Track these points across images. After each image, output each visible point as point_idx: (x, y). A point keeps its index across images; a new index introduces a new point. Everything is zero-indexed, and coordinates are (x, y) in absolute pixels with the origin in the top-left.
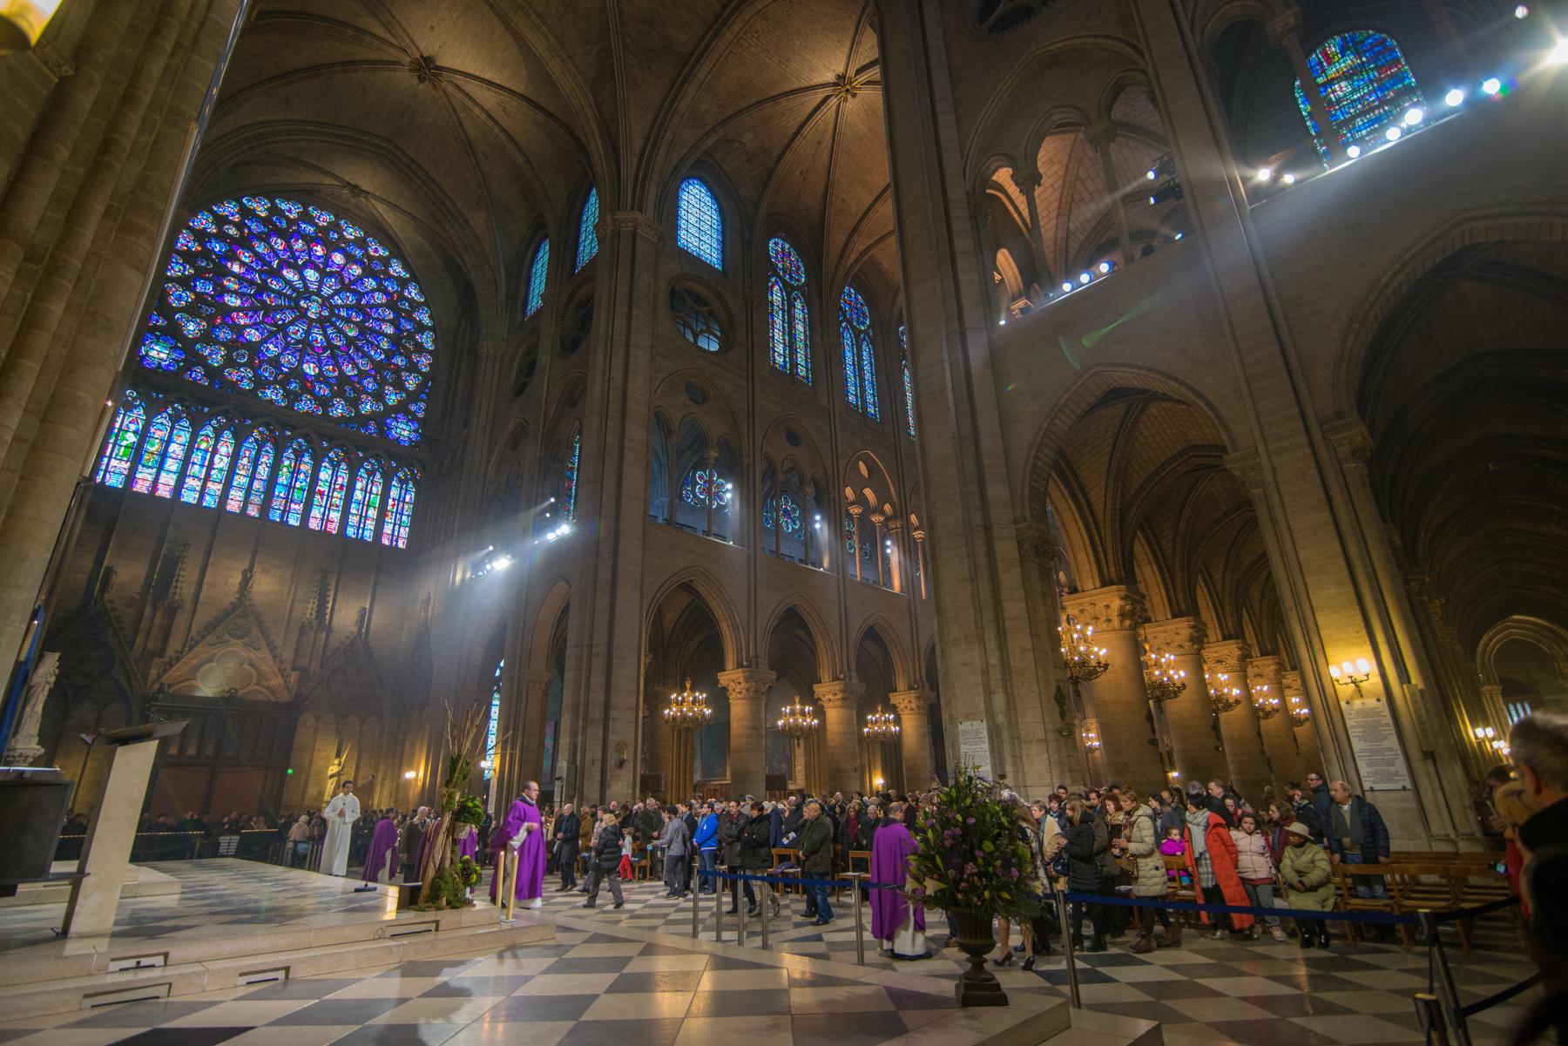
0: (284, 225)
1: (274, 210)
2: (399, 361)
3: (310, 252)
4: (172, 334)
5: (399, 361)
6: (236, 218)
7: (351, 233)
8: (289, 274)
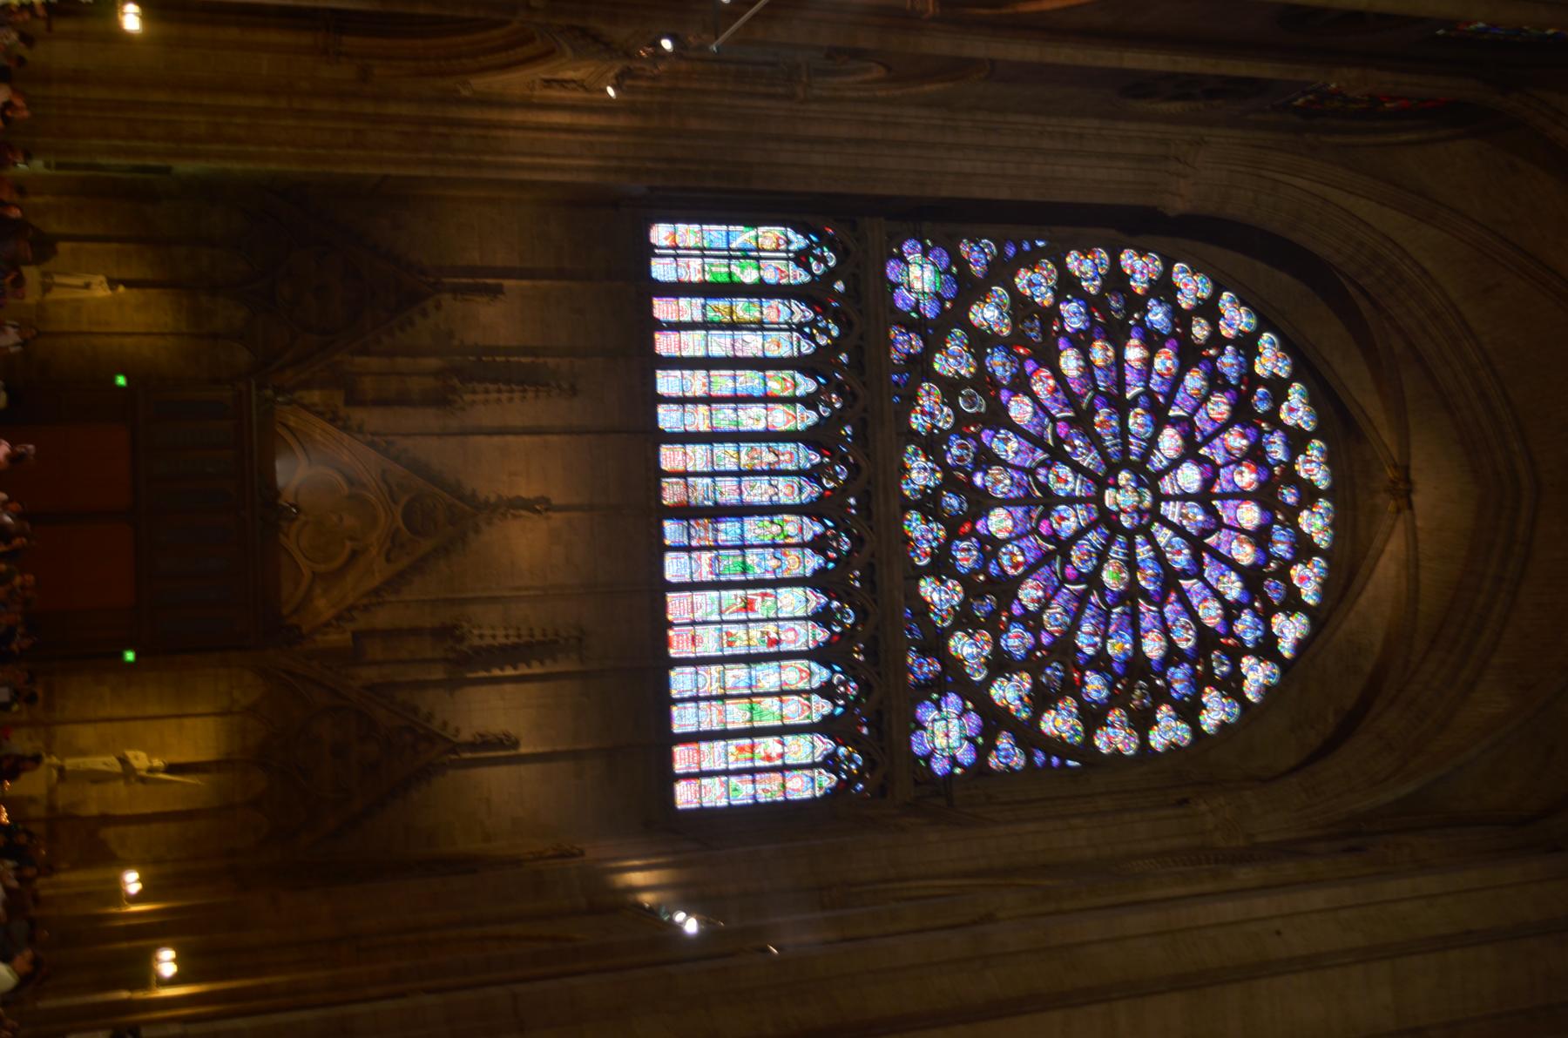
0: (1262, 408)
1: (1278, 389)
2: (1095, 685)
3: (1235, 461)
4: (967, 289)
5: (1095, 685)
6: (1226, 332)
7: (1314, 523)
8: (1170, 441)
